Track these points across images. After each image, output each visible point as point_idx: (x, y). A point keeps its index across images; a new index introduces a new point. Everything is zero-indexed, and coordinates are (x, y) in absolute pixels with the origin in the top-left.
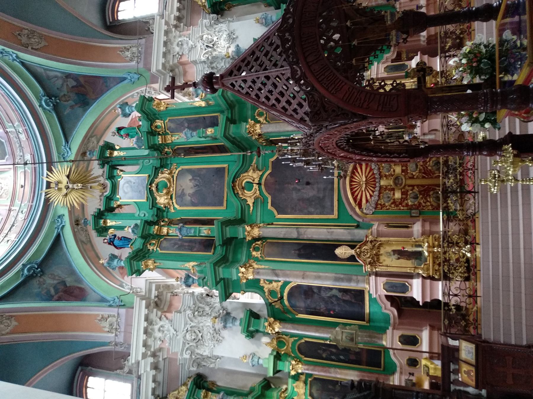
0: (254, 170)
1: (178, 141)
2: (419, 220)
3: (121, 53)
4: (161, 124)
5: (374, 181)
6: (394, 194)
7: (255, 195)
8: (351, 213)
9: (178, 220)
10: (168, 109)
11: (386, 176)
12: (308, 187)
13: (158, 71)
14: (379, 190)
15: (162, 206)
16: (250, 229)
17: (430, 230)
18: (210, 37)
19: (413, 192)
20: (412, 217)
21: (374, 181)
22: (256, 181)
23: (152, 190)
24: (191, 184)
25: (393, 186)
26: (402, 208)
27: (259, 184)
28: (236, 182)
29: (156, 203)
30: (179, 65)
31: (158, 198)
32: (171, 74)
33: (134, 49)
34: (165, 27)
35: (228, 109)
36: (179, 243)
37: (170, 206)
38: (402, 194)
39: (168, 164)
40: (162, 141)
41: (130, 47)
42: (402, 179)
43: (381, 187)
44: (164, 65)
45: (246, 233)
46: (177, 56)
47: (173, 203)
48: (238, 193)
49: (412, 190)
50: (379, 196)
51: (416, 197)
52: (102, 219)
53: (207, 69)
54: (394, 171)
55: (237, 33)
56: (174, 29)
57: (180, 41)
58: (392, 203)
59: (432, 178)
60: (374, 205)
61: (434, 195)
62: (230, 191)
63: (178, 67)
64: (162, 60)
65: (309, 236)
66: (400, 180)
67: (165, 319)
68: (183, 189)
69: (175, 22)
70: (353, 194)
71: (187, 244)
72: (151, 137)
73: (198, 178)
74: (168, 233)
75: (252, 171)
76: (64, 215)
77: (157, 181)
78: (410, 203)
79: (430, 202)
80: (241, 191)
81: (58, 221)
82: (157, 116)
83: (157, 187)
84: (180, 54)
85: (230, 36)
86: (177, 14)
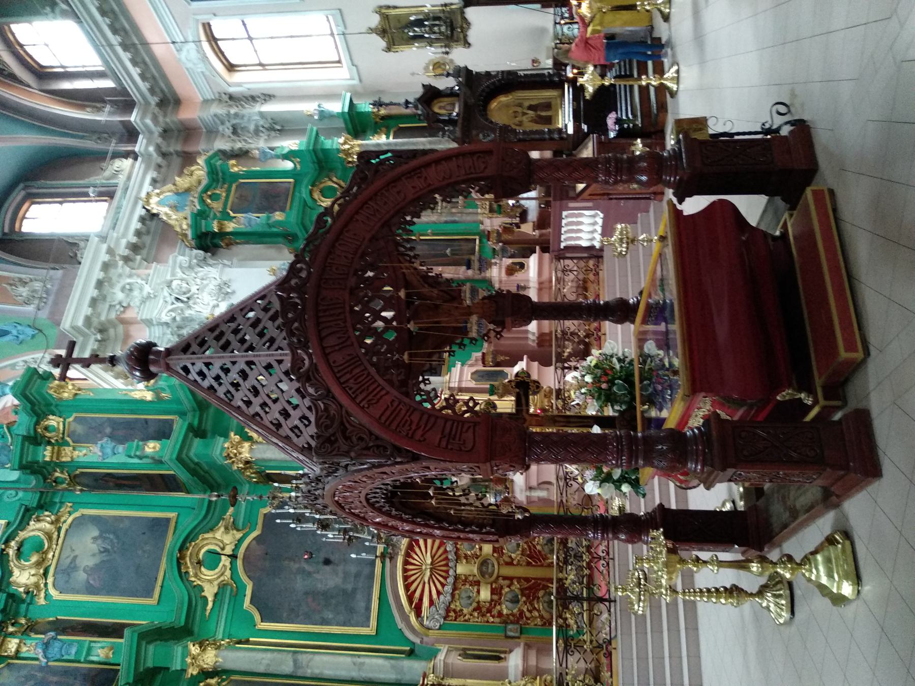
0: (226, 528)
1: (85, 459)
2: (518, 645)
3: (8, 287)
4: (58, 423)
5: (447, 565)
6: (478, 592)
7: (222, 578)
8: (401, 625)
9: (49, 623)
10: (78, 397)
11: (466, 557)
12: (327, 568)
13: (74, 328)
14: (454, 583)
15: (22, 590)
16: (198, 651)
17: (537, 667)
18: (185, 285)
19: (511, 591)
20: (507, 637)
21: (447, 565)
22: (228, 551)
23: (8, 554)
24: (94, 547)
25: (478, 578)
26: (491, 619)
27: (233, 557)
28: (188, 549)
29: (9, 584)
30: (117, 322)
31: (16, 572)
32: (99, 337)
33: (37, 285)
34: (105, 257)
35: (194, 410)
36: (39, 675)
37: (39, 591)
38: (492, 593)
39: (56, 503)
40: (52, 457)
41: (31, 280)
42: (493, 566)
43: (456, 578)
44: (88, 320)
45: (189, 660)
46: (118, 307)
47: (46, 584)
48: (187, 573)
49: (509, 586)
50: (453, 595)
51: (515, 601)
53: (170, 336)
54: (481, 549)
55: (234, 286)
56: (121, 263)
57: (129, 284)
58: (475, 610)
59: (542, 566)
60: (442, 612)
61: (546, 599)
62: (172, 568)
63: (115, 326)
64: (86, 310)
65: (317, 671)
66: (490, 566)
68: (76, 557)
69: (126, 252)
70: (407, 587)
71: (55, 679)
72: (31, 446)
73: (111, 536)
74: (17, 651)
75: (222, 529)
77: (22, 535)
78: (505, 612)
79: (539, 611)
80: (194, 568)
82: (53, 408)
83: (18, 549)
84: (125, 305)
85: (221, 289)
86: (134, 240)
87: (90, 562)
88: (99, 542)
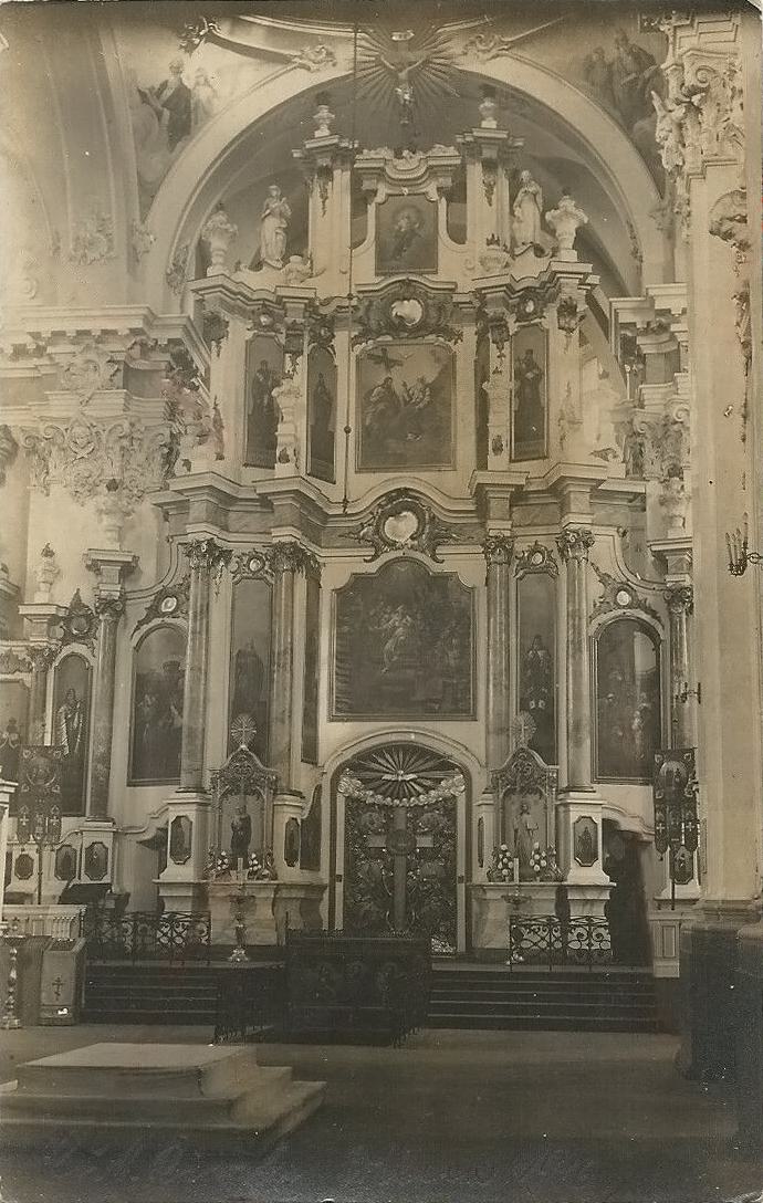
52: (333, 160)
54: (424, 834)
59: (407, 903)
67: (112, 372)
76: (334, 65)
81: (319, 52)
87: (397, 387)
88: (420, 386)
